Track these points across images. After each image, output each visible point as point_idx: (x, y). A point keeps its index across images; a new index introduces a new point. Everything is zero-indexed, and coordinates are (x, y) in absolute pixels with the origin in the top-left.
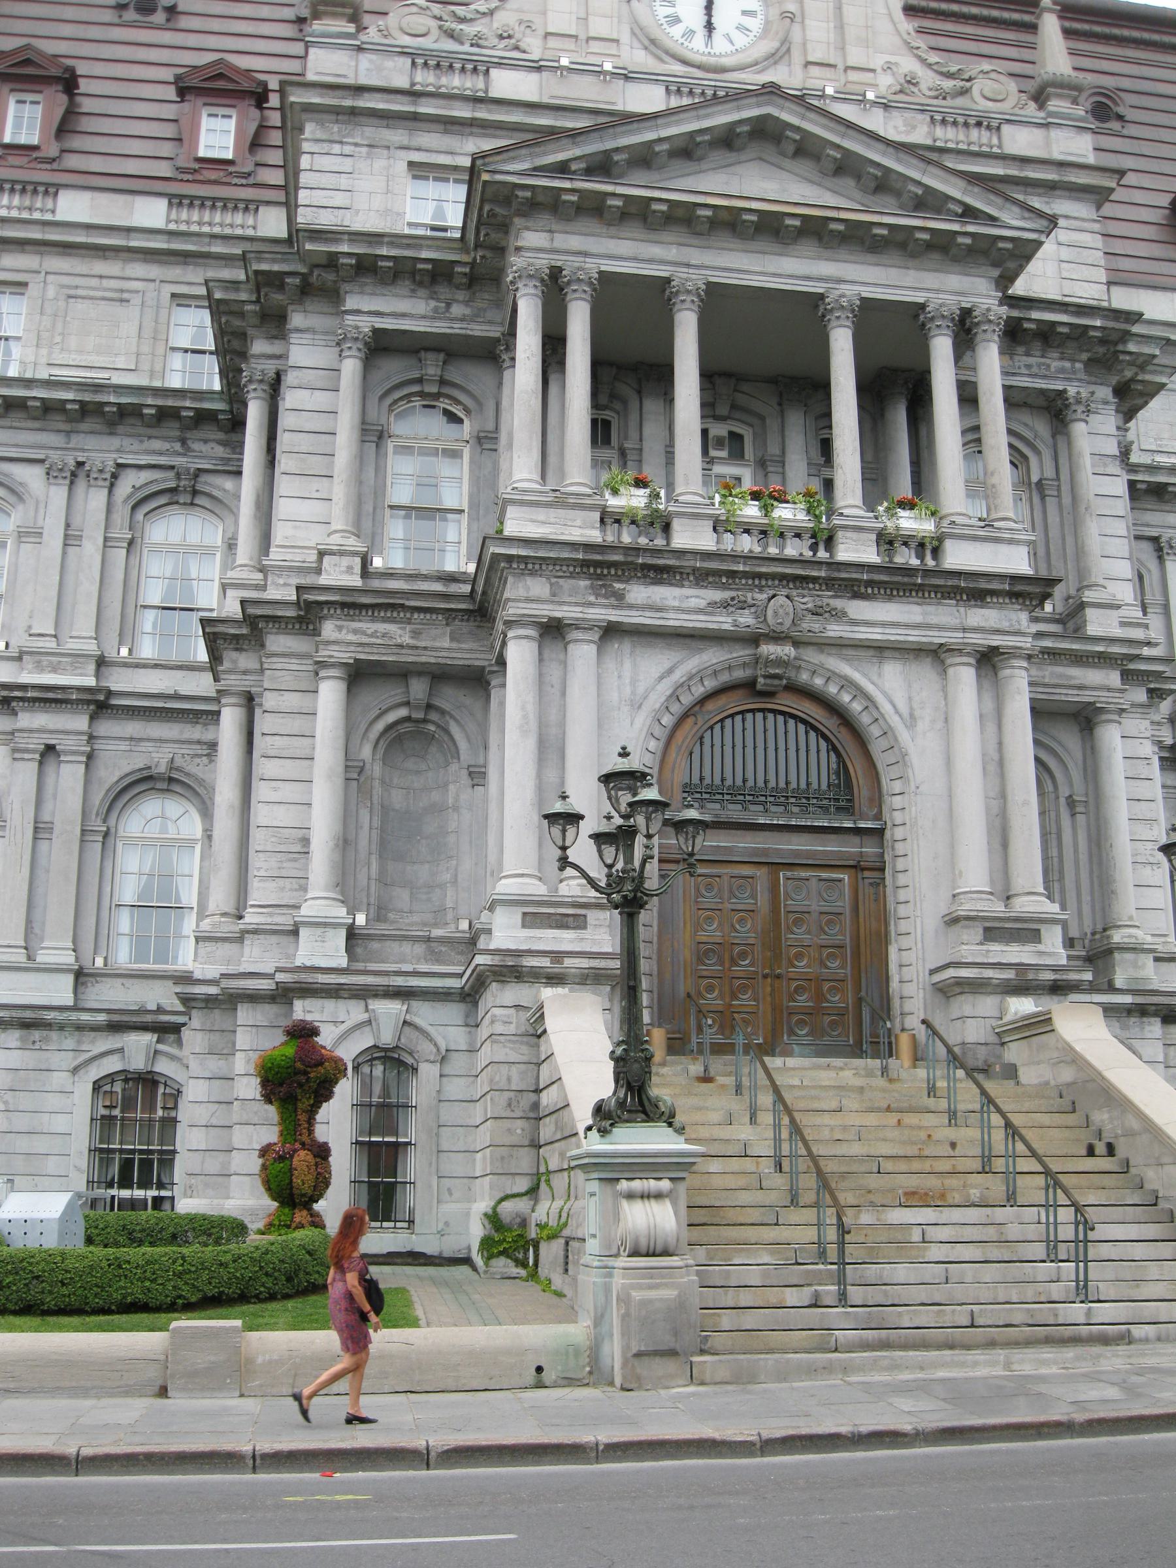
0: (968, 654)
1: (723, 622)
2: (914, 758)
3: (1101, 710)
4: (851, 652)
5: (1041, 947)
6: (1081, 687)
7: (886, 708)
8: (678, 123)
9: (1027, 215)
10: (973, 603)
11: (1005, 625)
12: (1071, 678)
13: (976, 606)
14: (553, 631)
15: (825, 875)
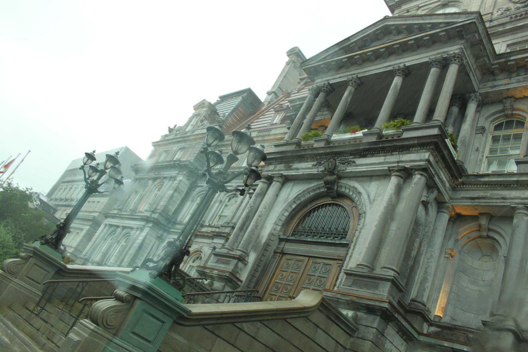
0: (397, 171)
1: (315, 171)
2: (368, 216)
3: (514, 209)
4: (361, 179)
5: (376, 292)
6: (504, 198)
7: (364, 196)
8: (356, 37)
9: (467, 16)
10: (405, 152)
11: (418, 158)
12: (498, 195)
13: (407, 153)
14: (270, 180)
15: (326, 261)
